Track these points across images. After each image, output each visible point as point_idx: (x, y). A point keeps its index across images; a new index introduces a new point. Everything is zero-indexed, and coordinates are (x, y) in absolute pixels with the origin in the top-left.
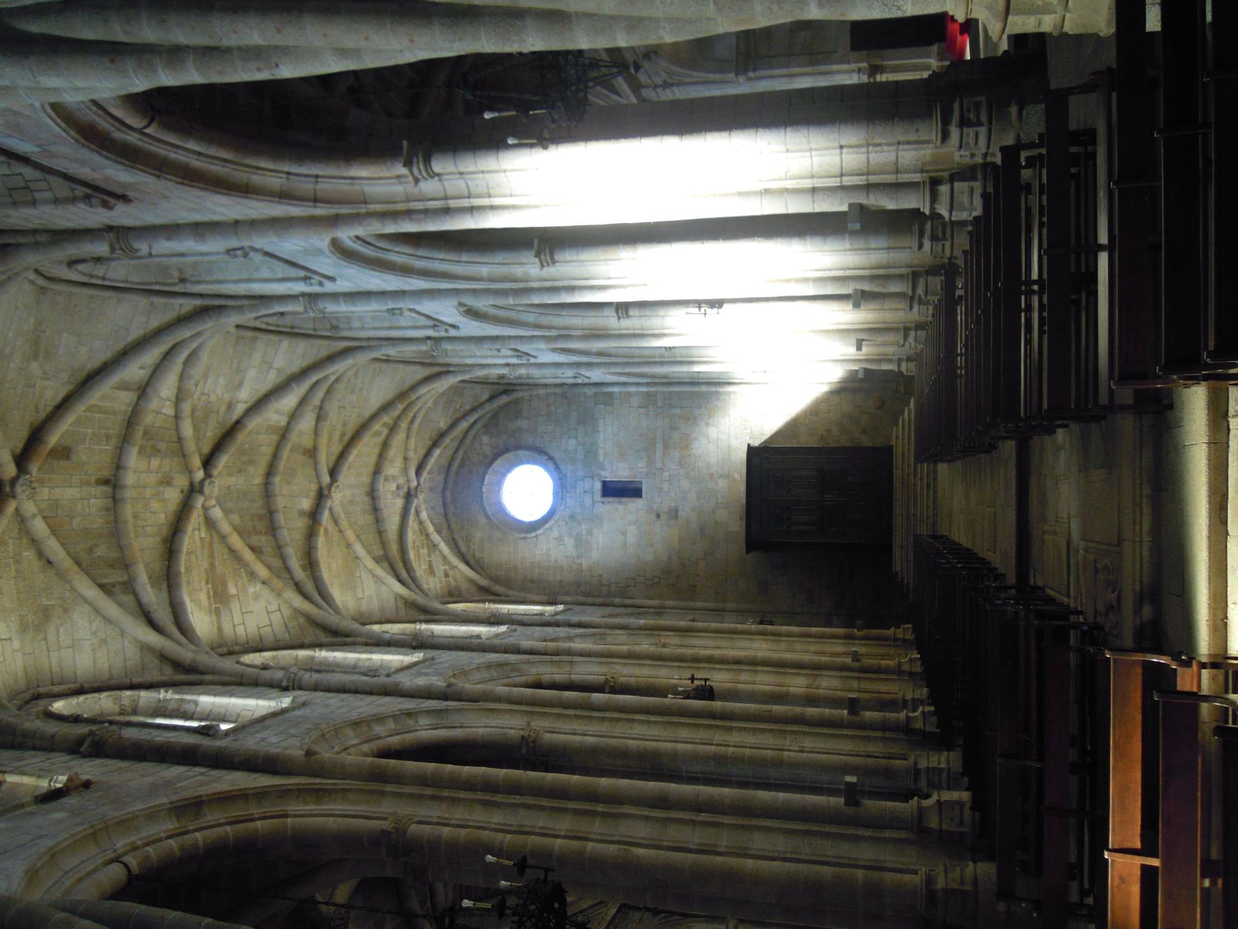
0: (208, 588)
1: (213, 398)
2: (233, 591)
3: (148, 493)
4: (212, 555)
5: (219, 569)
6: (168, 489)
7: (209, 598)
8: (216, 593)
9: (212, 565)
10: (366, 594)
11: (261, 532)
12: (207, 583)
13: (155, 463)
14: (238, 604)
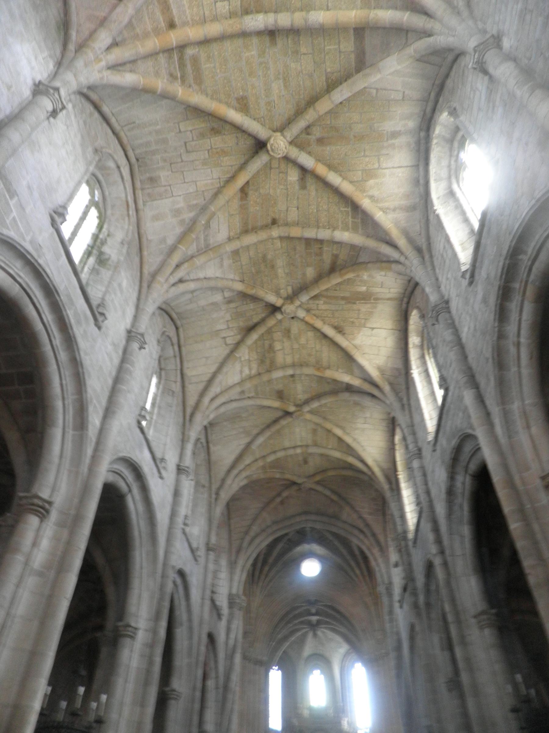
0: (359, 303)
1: (228, 317)
2: (364, 289)
3: (296, 346)
4: (336, 298)
5: (347, 294)
6: (292, 332)
7: (366, 303)
8: (364, 299)
9: (343, 298)
10: (400, 88)
11: (320, 248)
12: (355, 303)
13: (278, 346)
14: (374, 288)
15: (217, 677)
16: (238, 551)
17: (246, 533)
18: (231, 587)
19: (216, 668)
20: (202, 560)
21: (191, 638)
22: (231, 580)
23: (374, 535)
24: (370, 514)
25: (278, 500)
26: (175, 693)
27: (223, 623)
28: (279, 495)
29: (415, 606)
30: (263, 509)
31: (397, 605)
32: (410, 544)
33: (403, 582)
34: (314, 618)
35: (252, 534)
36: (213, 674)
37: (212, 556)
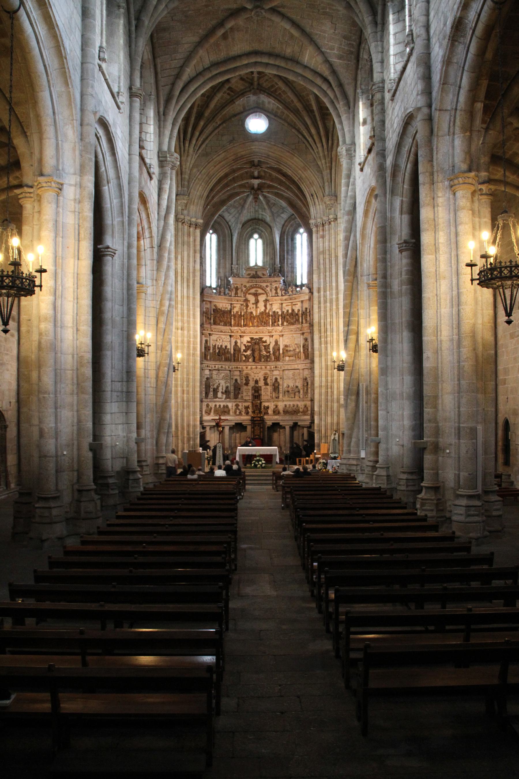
15: (151, 237)
16: (168, 101)
17: (178, 76)
18: (160, 144)
19: (150, 228)
20: (125, 108)
21: (121, 196)
22: (160, 134)
23: (341, 85)
24: (340, 57)
25: (220, 32)
26: (109, 250)
27: (154, 183)
28: (221, 24)
29: (381, 168)
30: (199, 44)
31: (358, 168)
32: (388, 96)
33: (369, 143)
34: (256, 182)
35: (185, 78)
36: (147, 234)
37: (137, 103)
